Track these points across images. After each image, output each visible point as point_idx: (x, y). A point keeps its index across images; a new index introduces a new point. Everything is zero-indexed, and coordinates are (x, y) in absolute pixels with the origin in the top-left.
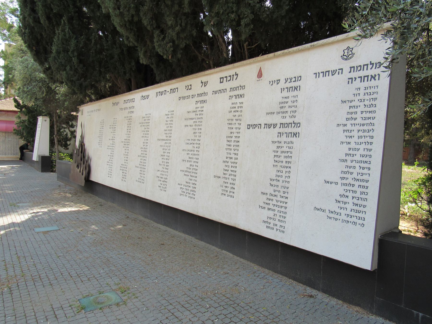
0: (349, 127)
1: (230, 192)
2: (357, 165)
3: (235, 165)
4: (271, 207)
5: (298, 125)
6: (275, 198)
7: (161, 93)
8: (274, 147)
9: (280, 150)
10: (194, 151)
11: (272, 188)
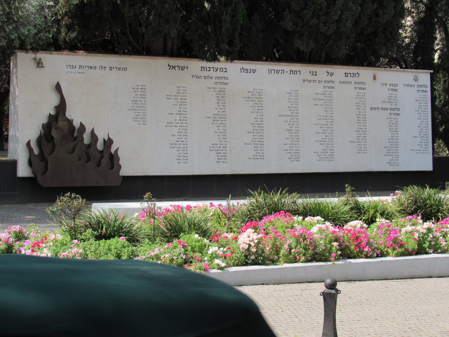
0: (419, 112)
1: (364, 150)
2: (424, 128)
3: (365, 133)
4: (391, 154)
5: (399, 109)
6: (392, 149)
7: (278, 72)
8: (388, 121)
9: (391, 123)
10: (327, 125)
11: (390, 144)
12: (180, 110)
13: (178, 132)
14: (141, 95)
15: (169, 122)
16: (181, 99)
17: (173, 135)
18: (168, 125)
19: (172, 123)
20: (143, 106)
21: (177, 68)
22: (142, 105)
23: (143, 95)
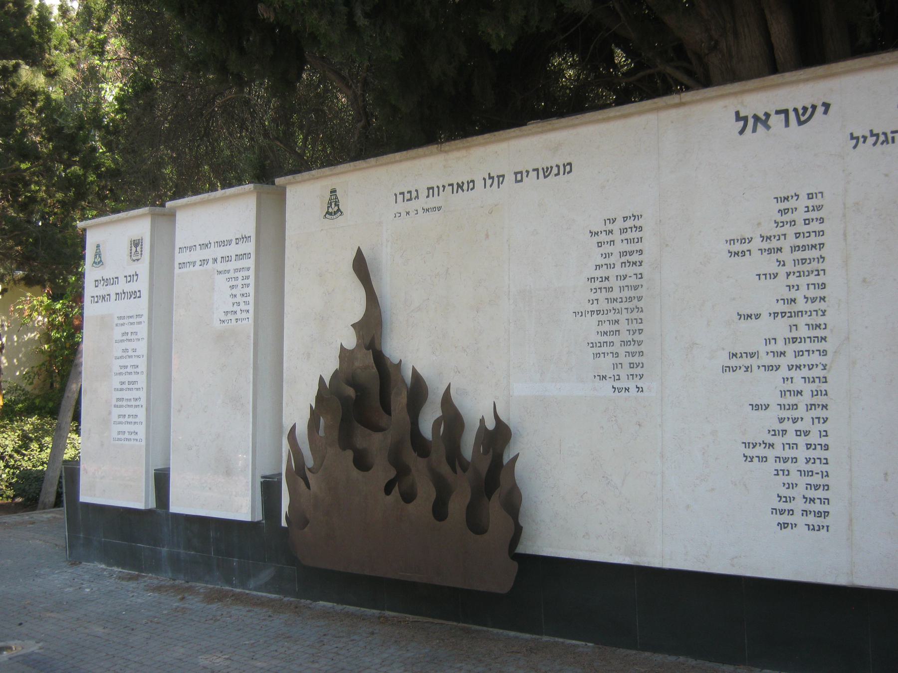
12: (793, 294)
13: (783, 393)
14: (623, 254)
15: (738, 350)
16: (795, 248)
17: (757, 407)
18: (734, 362)
19: (752, 355)
20: (632, 293)
21: (776, 121)
22: (627, 293)
23: (631, 253)
